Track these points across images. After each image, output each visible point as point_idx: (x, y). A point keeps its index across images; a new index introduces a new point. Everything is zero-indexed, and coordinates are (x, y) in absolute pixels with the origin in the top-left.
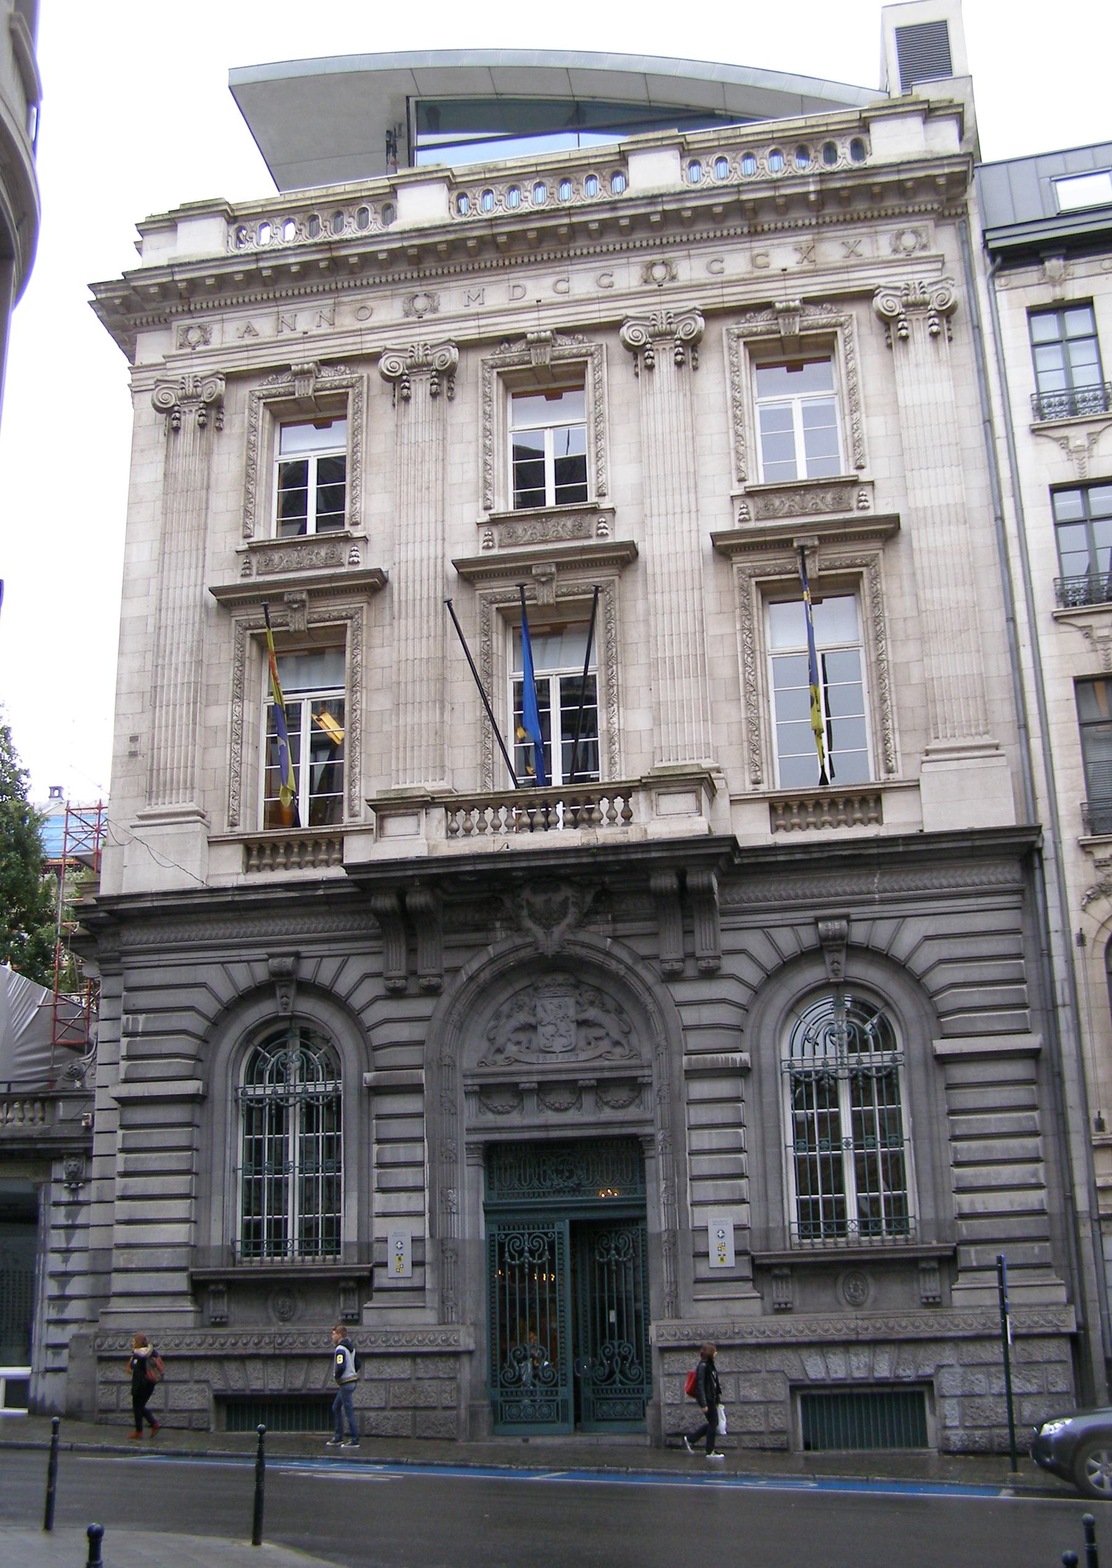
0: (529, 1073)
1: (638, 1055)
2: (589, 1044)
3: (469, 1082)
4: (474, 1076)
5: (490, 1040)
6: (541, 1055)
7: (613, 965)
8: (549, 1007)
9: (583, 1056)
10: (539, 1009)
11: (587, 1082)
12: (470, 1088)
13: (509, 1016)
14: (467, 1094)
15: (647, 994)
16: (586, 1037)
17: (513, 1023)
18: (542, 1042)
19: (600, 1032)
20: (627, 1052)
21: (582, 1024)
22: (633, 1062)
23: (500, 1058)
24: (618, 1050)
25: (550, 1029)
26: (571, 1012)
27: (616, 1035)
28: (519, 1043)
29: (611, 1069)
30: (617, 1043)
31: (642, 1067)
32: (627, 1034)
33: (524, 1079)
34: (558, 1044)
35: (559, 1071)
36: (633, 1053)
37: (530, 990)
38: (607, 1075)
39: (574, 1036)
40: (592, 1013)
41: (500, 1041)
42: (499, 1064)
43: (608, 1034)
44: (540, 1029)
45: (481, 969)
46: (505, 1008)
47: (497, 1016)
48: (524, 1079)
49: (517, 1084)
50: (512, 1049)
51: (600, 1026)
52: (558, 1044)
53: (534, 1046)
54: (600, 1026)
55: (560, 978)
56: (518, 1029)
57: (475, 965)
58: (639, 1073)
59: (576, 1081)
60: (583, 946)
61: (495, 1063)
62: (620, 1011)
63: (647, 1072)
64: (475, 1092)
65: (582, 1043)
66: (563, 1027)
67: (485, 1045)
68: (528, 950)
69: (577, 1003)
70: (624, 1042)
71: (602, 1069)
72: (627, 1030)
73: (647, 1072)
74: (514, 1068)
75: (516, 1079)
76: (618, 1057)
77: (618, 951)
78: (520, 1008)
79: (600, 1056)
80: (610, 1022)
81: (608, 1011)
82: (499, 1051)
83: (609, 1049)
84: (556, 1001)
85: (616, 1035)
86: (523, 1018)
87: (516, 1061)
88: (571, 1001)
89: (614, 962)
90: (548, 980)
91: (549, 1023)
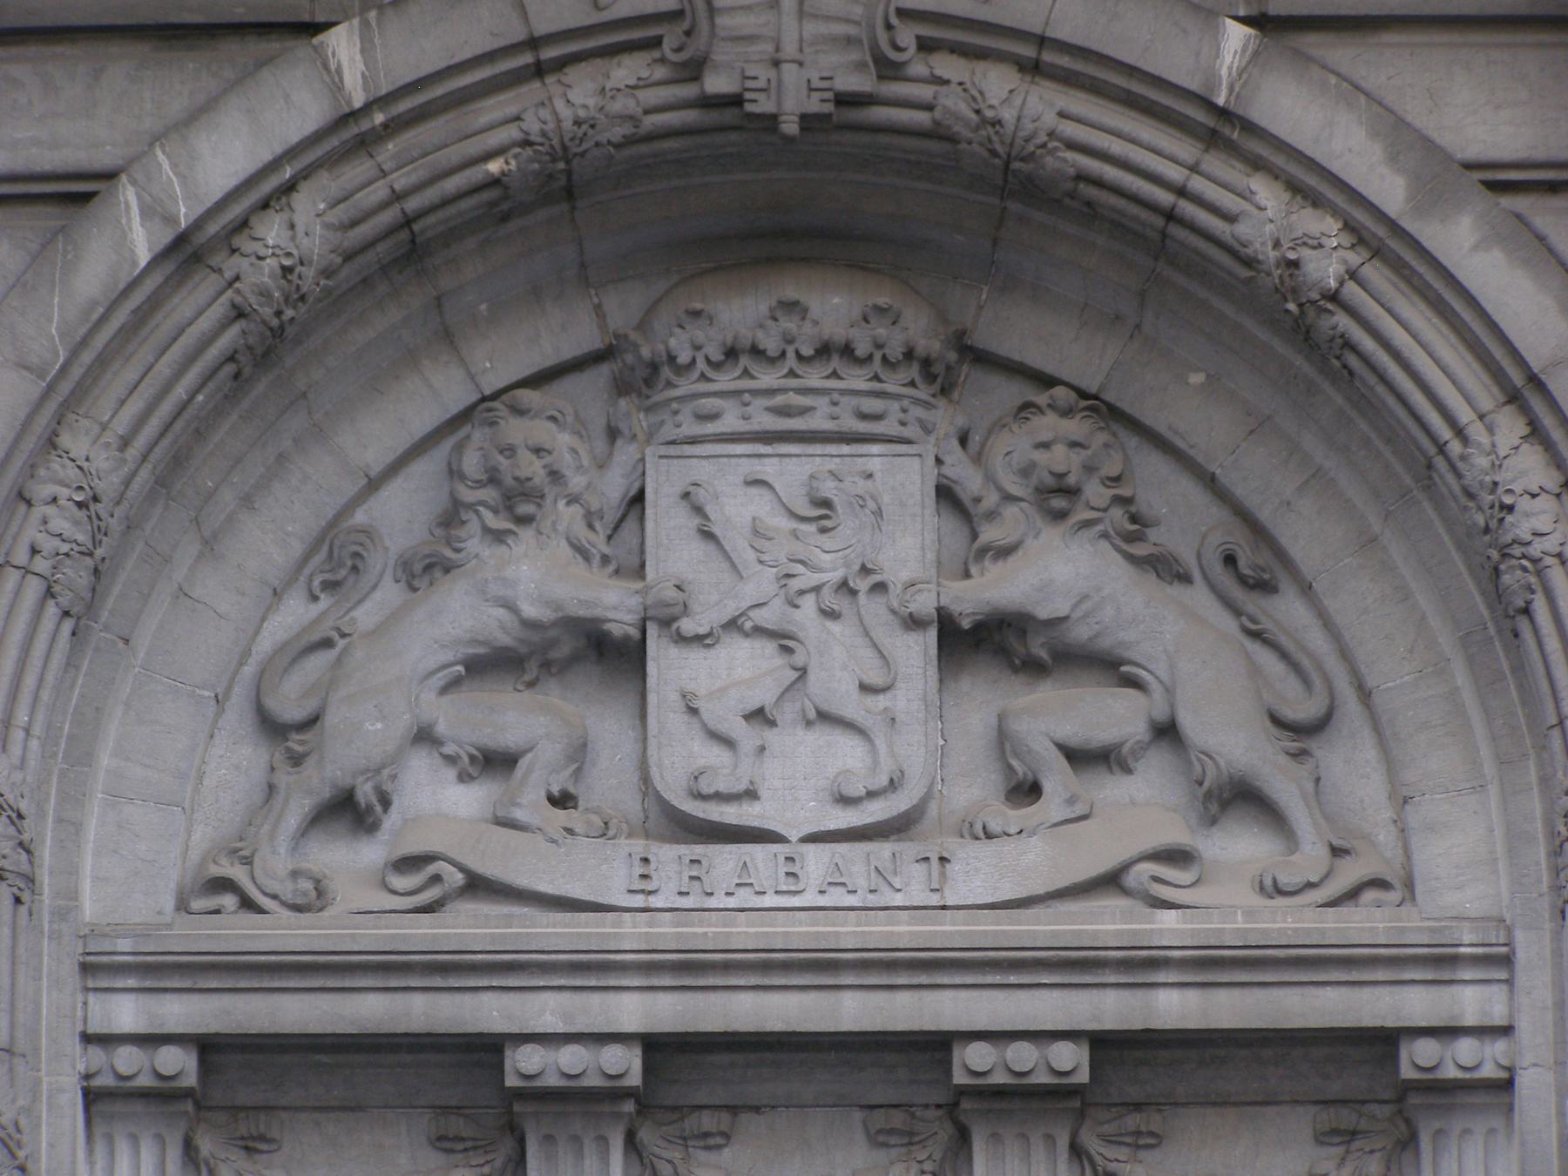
0: (592, 969)
1: (1396, 884)
2: (1026, 791)
3: (125, 1012)
4: (158, 972)
5: (272, 728)
6: (670, 857)
7: (1263, 215)
8: (736, 509)
9: (980, 874)
10: (666, 520)
11: (1023, 1056)
12: (127, 1059)
13: (426, 569)
14: (97, 1099)
15: (1510, 429)
16: (1003, 740)
17: (461, 615)
18: (681, 756)
19: (1111, 715)
20: (1311, 857)
21: (978, 642)
22: (1367, 923)
23: (348, 860)
24: (1239, 846)
25: (742, 669)
26: (910, 547)
27: (1232, 738)
28: (495, 762)
29: (1209, 965)
30: (1239, 798)
31: (1442, 963)
32: (1300, 734)
33: (546, 1010)
34: (797, 779)
35: (821, 967)
36: (1350, 873)
37: (590, 388)
38: (1173, 1007)
39: (931, 732)
40: (1057, 573)
41: (361, 734)
42: (355, 893)
43: (1167, 732)
44: (662, 658)
45: (271, 189)
46: (402, 514)
47: (336, 561)
48: (546, 1010)
49: (488, 1049)
50: (439, 806)
51: (1112, 668)
52: (797, 779)
53: (612, 784)
54: (1112, 668)
55: (833, 306)
56: (489, 665)
57: (224, 156)
58: (1412, 1004)
59: (936, 1046)
60: (1033, 69)
61: (315, 899)
62: (1253, 570)
63: (1472, 1001)
64: (163, 1095)
65: (973, 789)
66: (838, 658)
67: (237, 761)
68: (626, 70)
69: (946, 494)
70: (1285, 787)
71: (1139, 965)
72: (1303, 709)
73: (1472, 1001)
74: (471, 927)
75: (487, 1011)
76: (1234, 891)
77: (1292, 107)
78: (518, 503)
79: (1111, 881)
80: (1181, 640)
81: (1165, 568)
82: (348, 811)
83: (1175, 833)
84: (791, 471)
85: (1232, 738)
86: (539, 575)
87: (478, 886)
88: (903, 479)
89: (1267, 193)
90: (741, 311)
91: (732, 625)
